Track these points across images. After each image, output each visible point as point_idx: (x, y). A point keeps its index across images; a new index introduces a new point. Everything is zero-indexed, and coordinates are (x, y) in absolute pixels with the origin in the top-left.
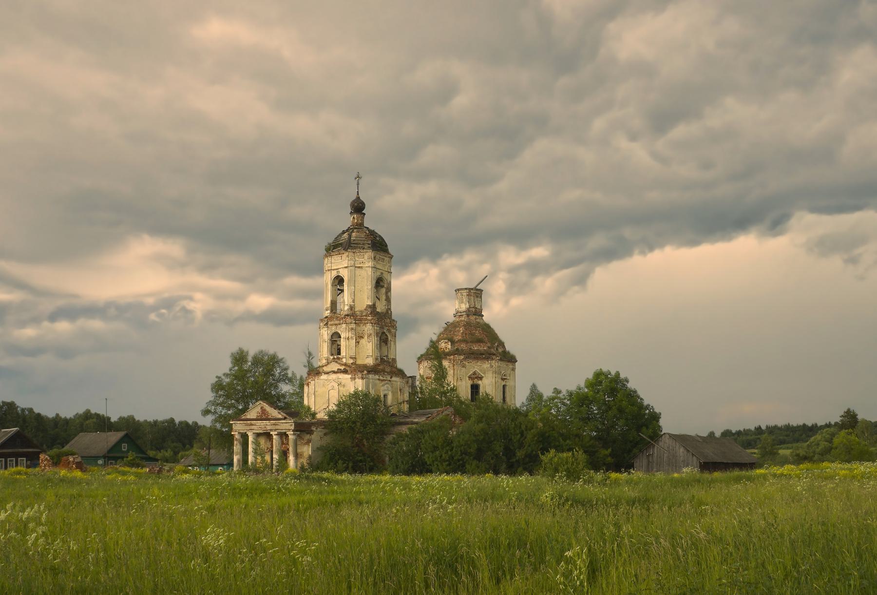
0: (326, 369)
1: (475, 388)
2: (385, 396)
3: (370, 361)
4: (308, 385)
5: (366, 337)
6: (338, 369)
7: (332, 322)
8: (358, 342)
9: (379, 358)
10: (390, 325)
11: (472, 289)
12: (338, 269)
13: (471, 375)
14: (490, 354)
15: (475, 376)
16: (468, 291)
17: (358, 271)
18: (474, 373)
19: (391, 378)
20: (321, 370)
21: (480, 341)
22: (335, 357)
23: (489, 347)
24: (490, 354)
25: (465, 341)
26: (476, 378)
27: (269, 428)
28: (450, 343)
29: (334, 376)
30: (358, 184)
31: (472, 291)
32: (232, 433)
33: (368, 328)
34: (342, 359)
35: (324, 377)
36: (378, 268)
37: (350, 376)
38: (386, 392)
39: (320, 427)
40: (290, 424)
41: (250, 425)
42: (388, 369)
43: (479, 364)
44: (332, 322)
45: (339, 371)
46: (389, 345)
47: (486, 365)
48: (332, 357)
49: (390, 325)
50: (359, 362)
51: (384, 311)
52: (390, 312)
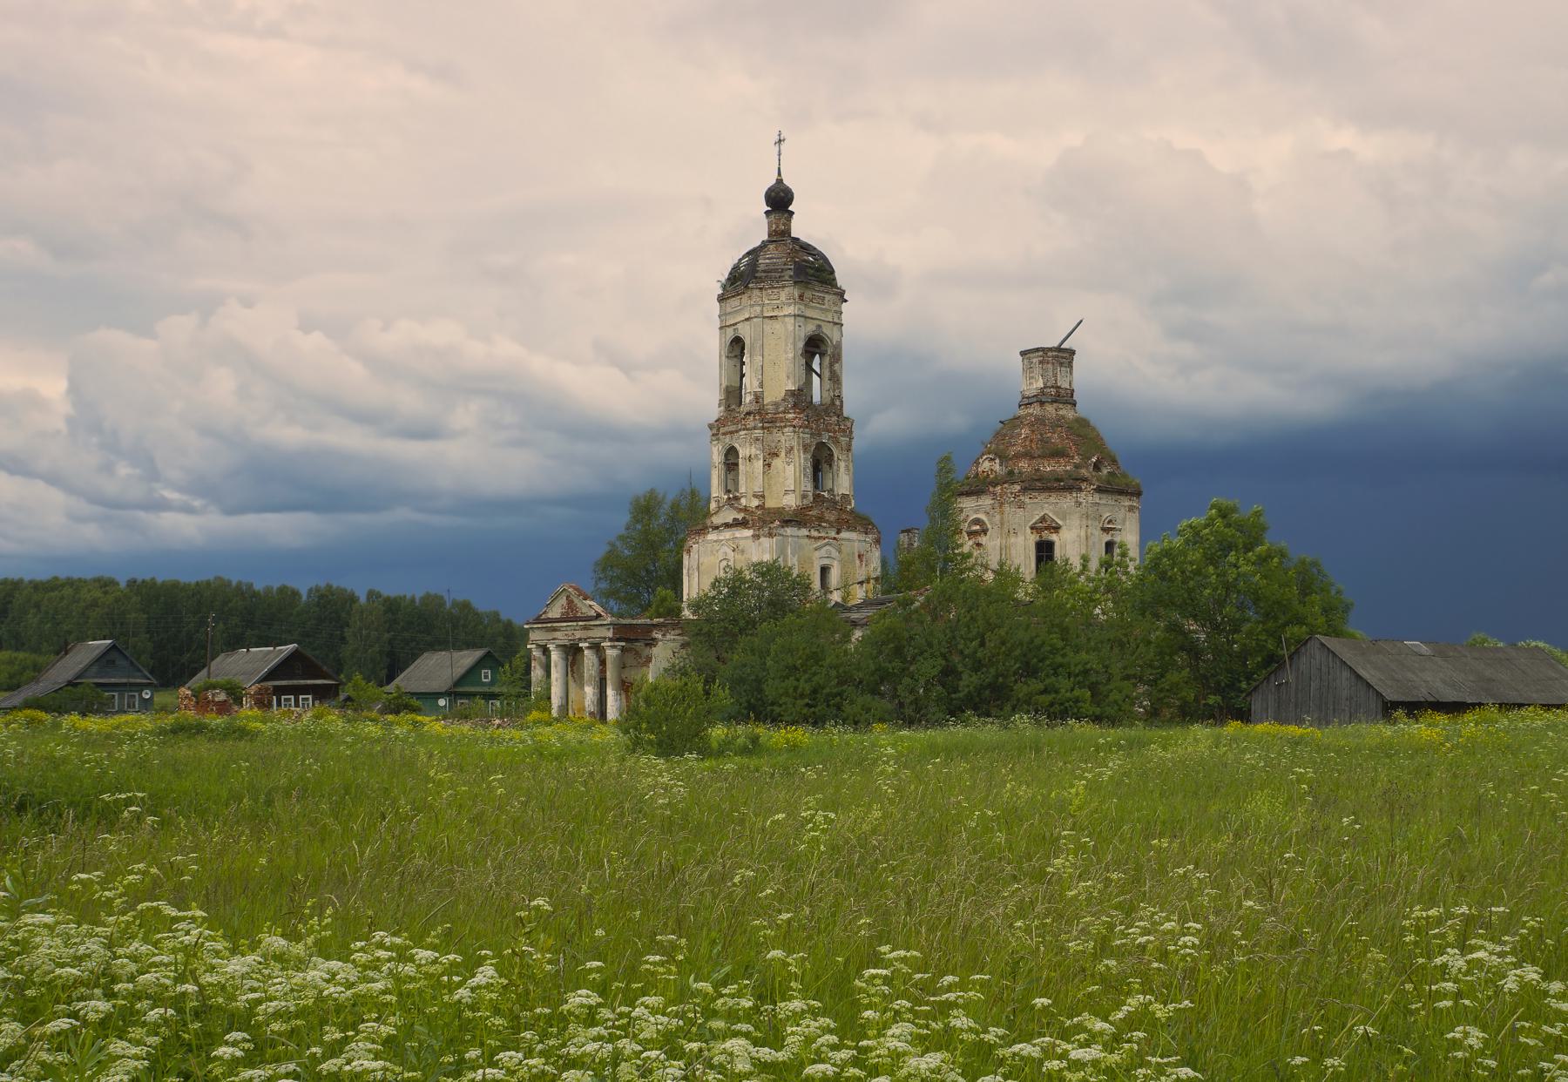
0: (717, 520)
1: (1045, 551)
2: (825, 571)
3: (791, 502)
4: (689, 552)
5: (783, 454)
6: (735, 519)
7: (726, 429)
8: (769, 465)
9: (810, 494)
10: (837, 428)
11: (1050, 349)
12: (736, 324)
13: (1036, 523)
14: (1077, 480)
15: (1047, 525)
16: (1041, 353)
17: (769, 326)
18: (1043, 519)
19: (838, 533)
21: (1058, 454)
23: (1077, 466)
24: (1077, 480)
25: (1028, 455)
26: (1046, 528)
27: (578, 634)
28: (997, 461)
31: (1050, 354)
32: (529, 646)
33: (786, 438)
35: (712, 536)
36: (810, 316)
37: (749, 533)
38: (826, 562)
39: (673, 632)
41: (553, 631)
42: (831, 516)
43: (1052, 499)
44: (726, 429)
45: (738, 524)
46: (835, 468)
47: (1067, 501)
48: (726, 497)
49: (837, 428)
50: (771, 503)
51: (828, 401)
52: (838, 403)
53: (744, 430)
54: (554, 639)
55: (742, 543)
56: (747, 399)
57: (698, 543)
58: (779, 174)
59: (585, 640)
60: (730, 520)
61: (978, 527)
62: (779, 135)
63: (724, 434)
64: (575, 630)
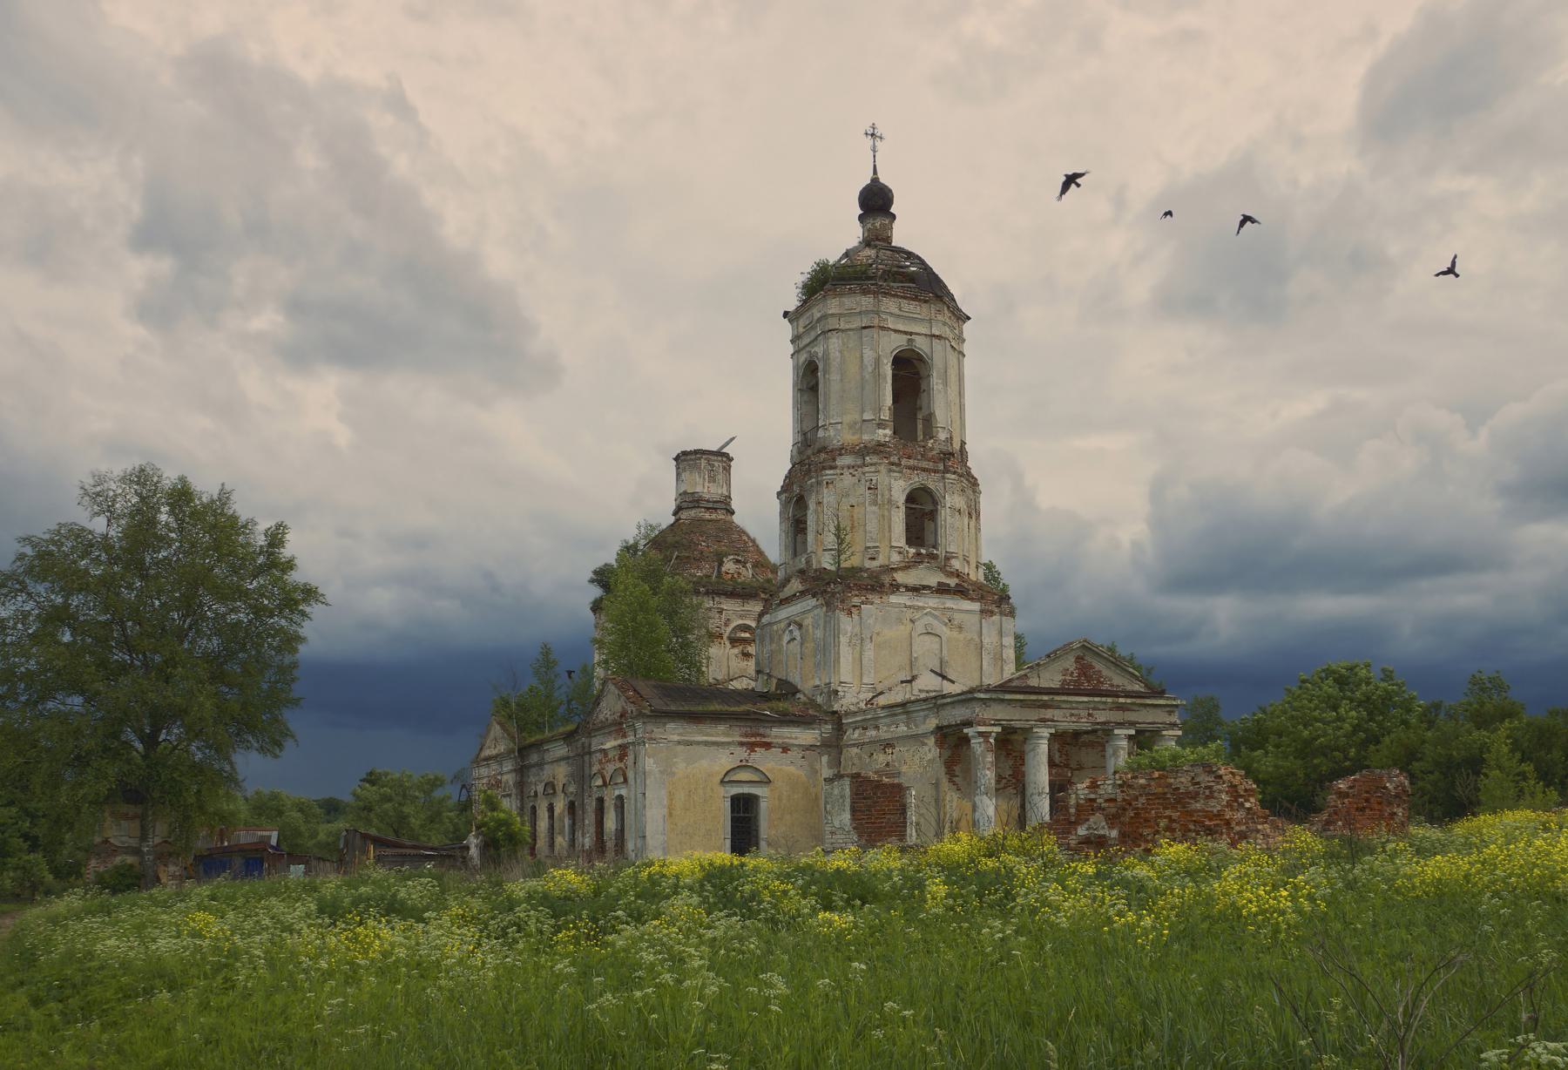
0: (900, 577)
6: (939, 584)
7: (911, 462)
12: (911, 334)
20: (886, 579)
22: (923, 551)
27: (1101, 717)
29: (932, 602)
30: (874, 156)
34: (947, 559)
37: (976, 606)
40: (1168, 709)
41: (1039, 707)
44: (911, 462)
45: (942, 590)
53: (954, 473)
54: (1043, 720)
55: (958, 617)
56: (942, 436)
57: (872, 603)
58: (875, 172)
59: (1132, 724)
60: (933, 579)
61: (747, 635)
62: (874, 129)
63: (909, 468)
64: (1094, 709)
